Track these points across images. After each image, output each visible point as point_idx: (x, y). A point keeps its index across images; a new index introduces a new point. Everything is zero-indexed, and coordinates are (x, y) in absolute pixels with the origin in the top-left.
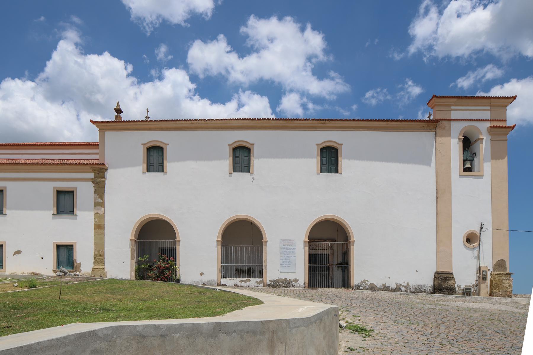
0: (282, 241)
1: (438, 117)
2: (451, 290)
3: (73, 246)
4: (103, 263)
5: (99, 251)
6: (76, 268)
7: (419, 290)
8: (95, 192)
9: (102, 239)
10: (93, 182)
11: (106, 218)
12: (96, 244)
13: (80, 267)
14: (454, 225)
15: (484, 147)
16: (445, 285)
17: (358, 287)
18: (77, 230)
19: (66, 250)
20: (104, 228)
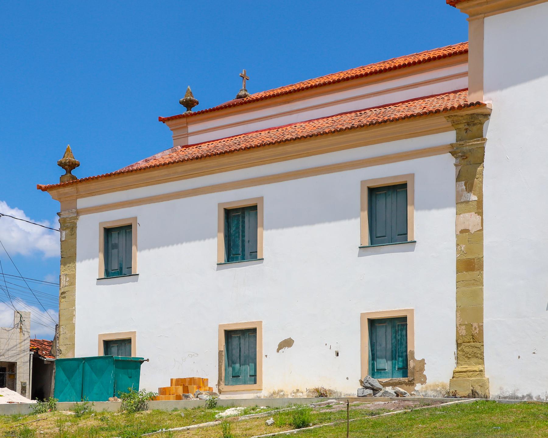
4: (479, 357)
5: (469, 326)
6: (413, 374)
8: (458, 179)
9: (478, 296)
10: (453, 153)
11: (486, 241)
12: (460, 310)
13: (422, 369)
19: (389, 330)
20: (481, 268)
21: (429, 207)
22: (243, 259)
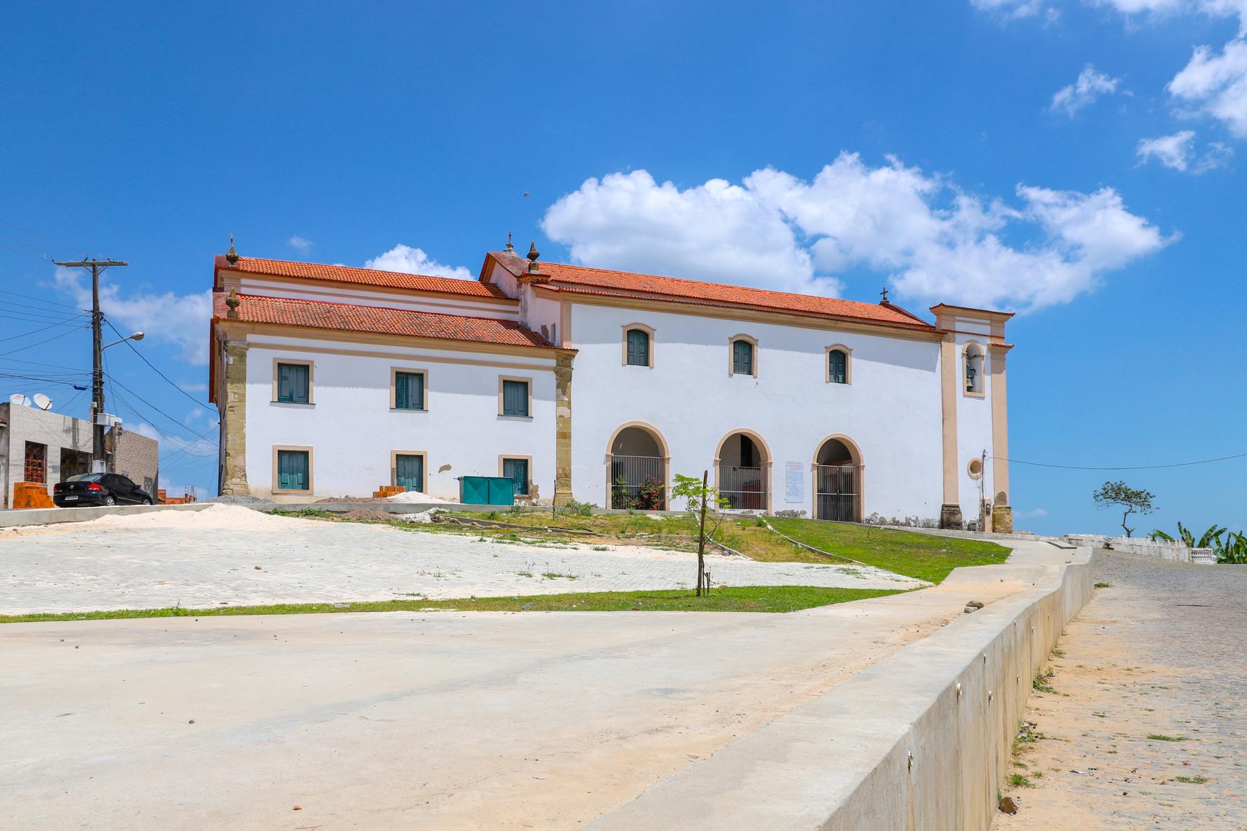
0: (788, 464)
1: (944, 327)
2: (958, 525)
3: (526, 461)
4: (568, 486)
5: (564, 469)
7: (927, 525)
9: (568, 453)
14: (960, 452)
15: (984, 364)
16: (953, 519)
17: (868, 521)
18: (532, 439)
21: (541, 398)
22: (407, 407)
